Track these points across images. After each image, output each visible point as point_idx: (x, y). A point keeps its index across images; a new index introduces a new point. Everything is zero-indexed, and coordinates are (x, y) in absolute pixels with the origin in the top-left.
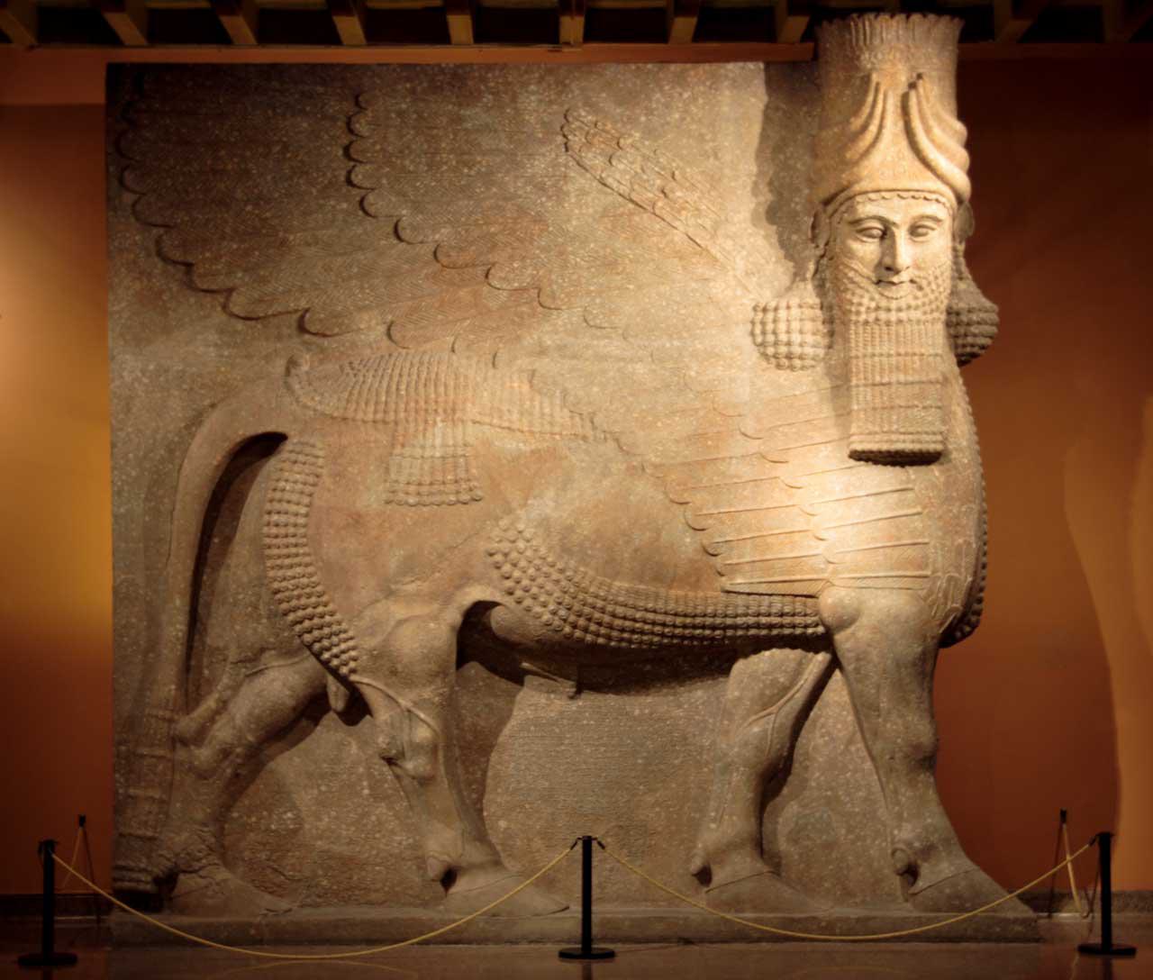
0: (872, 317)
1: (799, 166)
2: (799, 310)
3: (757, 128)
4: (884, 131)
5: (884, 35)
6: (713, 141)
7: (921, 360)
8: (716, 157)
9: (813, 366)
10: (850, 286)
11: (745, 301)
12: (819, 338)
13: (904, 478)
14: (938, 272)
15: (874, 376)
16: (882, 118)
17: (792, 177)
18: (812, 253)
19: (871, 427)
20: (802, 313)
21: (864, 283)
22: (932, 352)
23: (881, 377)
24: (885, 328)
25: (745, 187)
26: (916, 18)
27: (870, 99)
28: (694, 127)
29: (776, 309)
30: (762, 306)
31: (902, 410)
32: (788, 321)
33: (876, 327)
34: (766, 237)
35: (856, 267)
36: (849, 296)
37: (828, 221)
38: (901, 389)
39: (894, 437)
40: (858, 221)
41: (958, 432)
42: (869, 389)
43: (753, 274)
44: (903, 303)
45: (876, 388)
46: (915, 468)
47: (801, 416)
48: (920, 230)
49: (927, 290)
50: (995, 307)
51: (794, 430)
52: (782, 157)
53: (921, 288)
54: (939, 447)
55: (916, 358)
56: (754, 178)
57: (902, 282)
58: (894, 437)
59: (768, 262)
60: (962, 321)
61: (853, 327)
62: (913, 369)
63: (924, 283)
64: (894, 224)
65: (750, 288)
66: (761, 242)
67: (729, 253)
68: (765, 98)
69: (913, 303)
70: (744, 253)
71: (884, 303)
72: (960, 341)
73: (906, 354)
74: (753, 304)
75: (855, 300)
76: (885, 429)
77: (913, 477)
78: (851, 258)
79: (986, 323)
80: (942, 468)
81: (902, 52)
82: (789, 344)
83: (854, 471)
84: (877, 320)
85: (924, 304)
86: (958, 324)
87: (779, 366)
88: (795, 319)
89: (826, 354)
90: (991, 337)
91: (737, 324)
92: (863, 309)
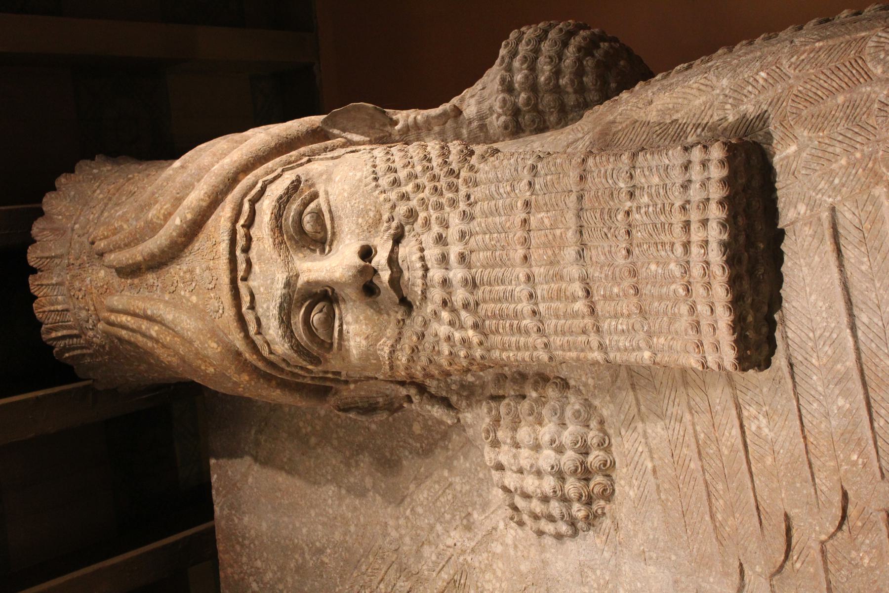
0: (467, 318)
1: (322, 413)
2: (505, 448)
3: (282, 478)
4: (149, 312)
5: (59, 307)
6: (303, 554)
7: (539, 209)
8: (321, 551)
9: (602, 422)
10: (424, 361)
11: (509, 540)
12: (545, 412)
13: (808, 231)
14: (384, 182)
15: (575, 315)
16: (134, 315)
17: (338, 426)
18: (419, 406)
19: (684, 322)
20: (505, 443)
21: (409, 339)
22: (524, 184)
23: (575, 299)
24: (480, 293)
25: (355, 509)
26: (33, 256)
27: (124, 333)
28: (289, 579)
29: (506, 489)
30: (510, 512)
31: (636, 251)
32: (521, 471)
33: (483, 308)
34: (419, 481)
35: (387, 350)
36: (444, 362)
37: (352, 386)
38: (594, 254)
39: (696, 271)
40: (298, 348)
41: (697, 102)
42: (605, 326)
43: (469, 514)
44: (432, 253)
45: (599, 308)
46: (780, 206)
47: (692, 466)
48: (308, 227)
49: (414, 203)
50: (513, 35)
51: (720, 486)
52: (313, 440)
53: (412, 215)
54: (717, 152)
55: (533, 221)
56: (343, 492)
57: (392, 261)
58: (696, 271)
59: (451, 484)
60: (528, 102)
61: (496, 354)
62: (553, 227)
63: (402, 209)
64: (288, 284)
65: (488, 525)
66: (422, 496)
67: (439, 555)
68: (248, 459)
69: (436, 229)
70: (439, 528)
71: (436, 294)
72: (571, 100)
73: (526, 242)
74: (513, 524)
75: (445, 349)
76: (682, 292)
77: (802, 208)
78: (377, 358)
79: (537, 51)
80: (776, 137)
81: (73, 277)
82: (560, 476)
83: (798, 357)
84: (466, 306)
85: (439, 207)
86: (535, 108)
87: (608, 495)
88: (515, 457)
89: (578, 391)
90: (571, 34)
91: (545, 563)
92: (457, 335)
